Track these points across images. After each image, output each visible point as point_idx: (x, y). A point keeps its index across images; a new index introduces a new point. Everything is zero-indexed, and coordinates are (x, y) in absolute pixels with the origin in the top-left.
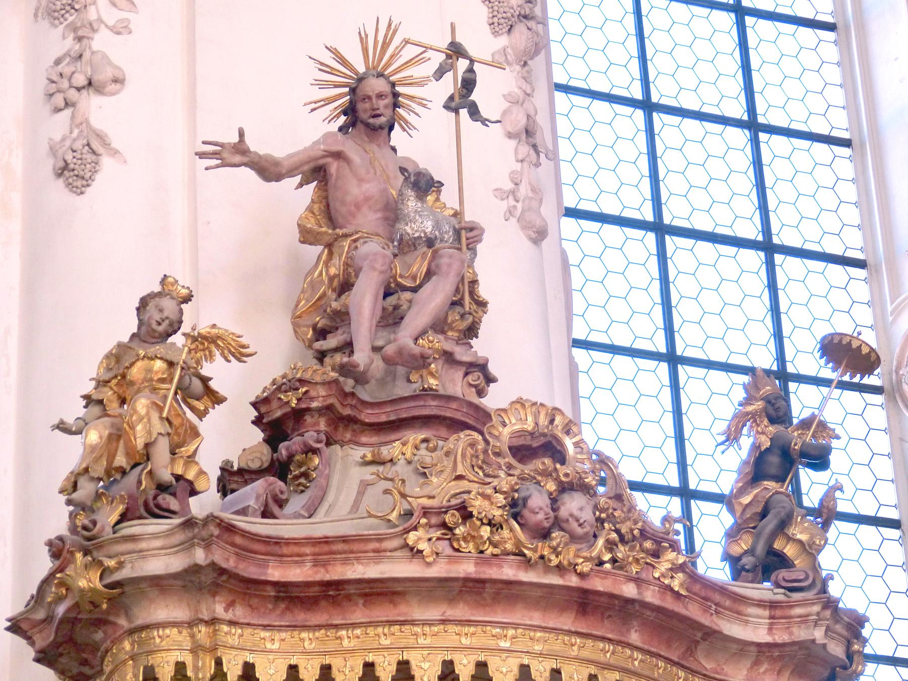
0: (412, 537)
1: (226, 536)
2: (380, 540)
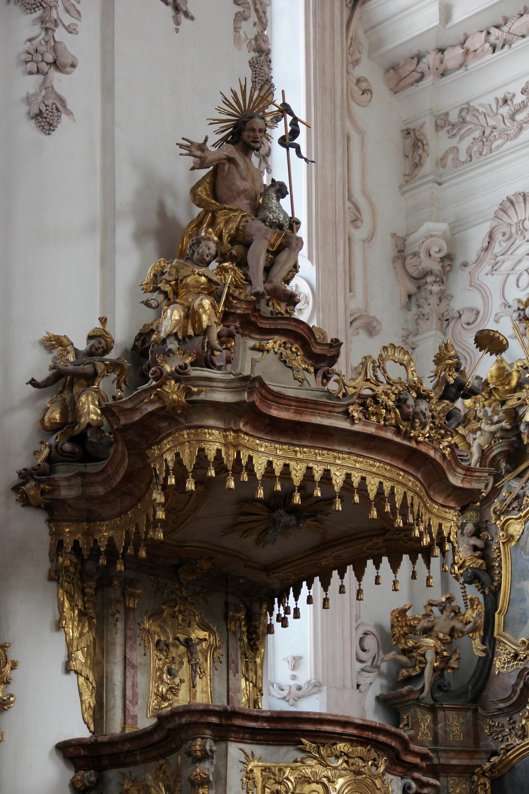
0: (351, 408)
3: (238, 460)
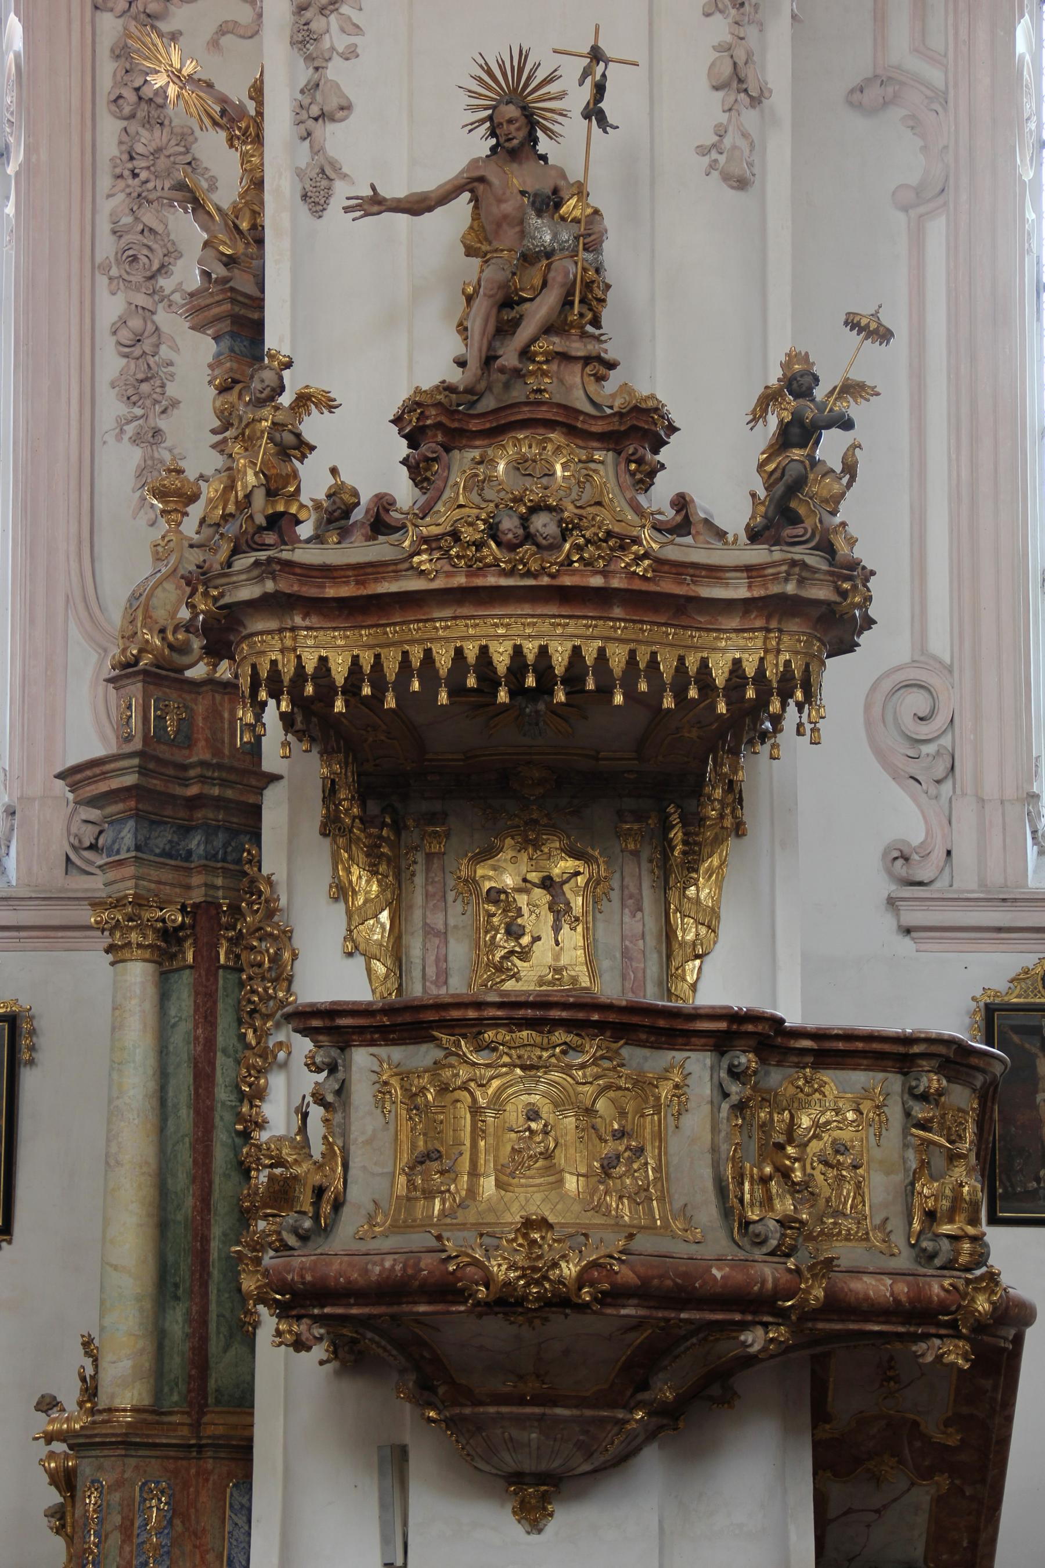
1: (287, 569)
2: (396, 564)
3: (300, 667)
